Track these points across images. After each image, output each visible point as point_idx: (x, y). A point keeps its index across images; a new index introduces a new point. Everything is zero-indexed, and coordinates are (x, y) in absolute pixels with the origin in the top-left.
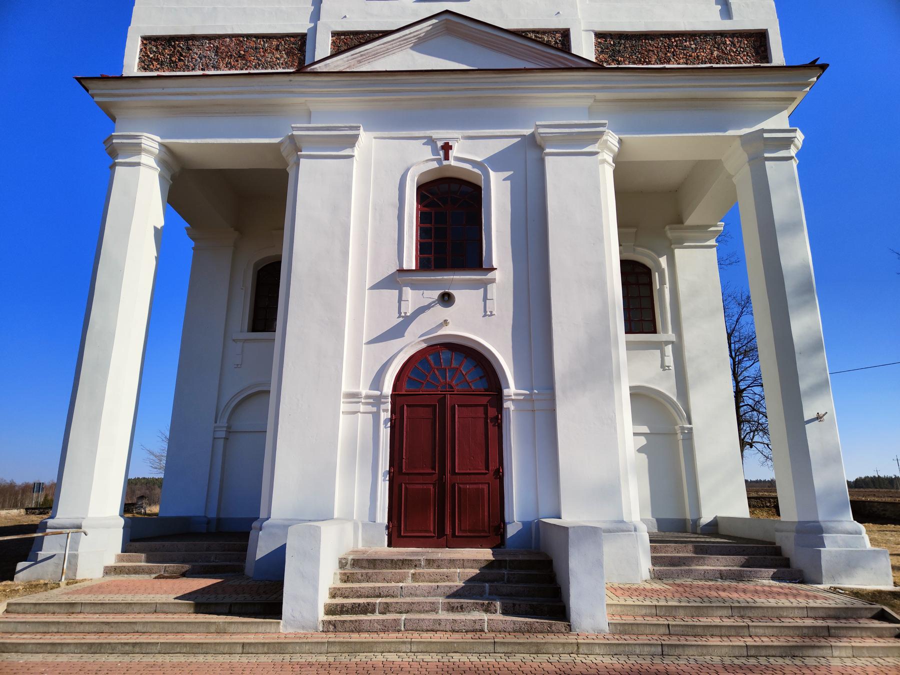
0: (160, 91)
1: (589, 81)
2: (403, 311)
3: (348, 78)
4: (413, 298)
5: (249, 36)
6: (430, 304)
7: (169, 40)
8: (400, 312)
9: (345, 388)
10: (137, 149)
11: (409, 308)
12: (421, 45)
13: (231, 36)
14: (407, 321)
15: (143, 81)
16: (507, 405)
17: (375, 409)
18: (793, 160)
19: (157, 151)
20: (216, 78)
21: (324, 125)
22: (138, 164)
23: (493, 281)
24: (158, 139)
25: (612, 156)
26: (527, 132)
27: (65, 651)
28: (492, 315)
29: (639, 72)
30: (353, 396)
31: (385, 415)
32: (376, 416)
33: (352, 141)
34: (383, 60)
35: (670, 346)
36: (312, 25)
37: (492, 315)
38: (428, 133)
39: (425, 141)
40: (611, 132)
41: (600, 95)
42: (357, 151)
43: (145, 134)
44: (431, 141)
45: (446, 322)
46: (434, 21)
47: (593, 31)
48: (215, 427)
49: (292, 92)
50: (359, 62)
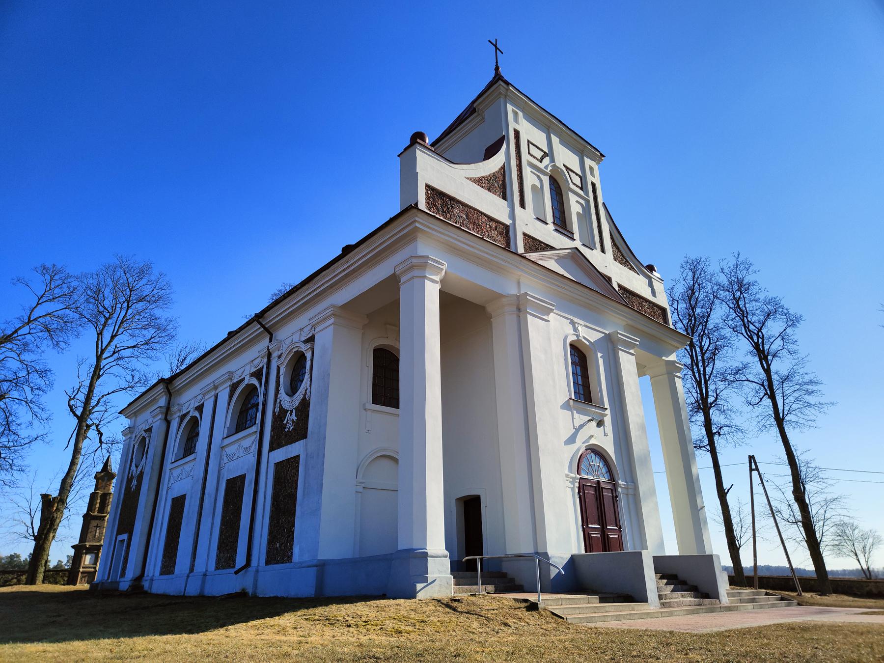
0: (456, 237)
2: (575, 425)
3: (545, 271)
4: (580, 419)
5: (482, 213)
6: (584, 424)
7: (441, 195)
8: (574, 426)
11: (577, 425)
12: (560, 260)
13: (474, 209)
14: (577, 430)
16: (620, 490)
17: (572, 486)
20: (488, 243)
21: (533, 295)
23: (606, 415)
26: (607, 332)
27: (609, 619)
28: (607, 436)
29: (637, 314)
31: (577, 490)
32: (573, 489)
33: (548, 311)
34: (547, 262)
36: (511, 222)
37: (607, 436)
38: (576, 320)
39: (570, 321)
44: (572, 323)
45: (592, 436)
46: (569, 251)
48: (357, 482)
49: (518, 268)
50: (540, 259)
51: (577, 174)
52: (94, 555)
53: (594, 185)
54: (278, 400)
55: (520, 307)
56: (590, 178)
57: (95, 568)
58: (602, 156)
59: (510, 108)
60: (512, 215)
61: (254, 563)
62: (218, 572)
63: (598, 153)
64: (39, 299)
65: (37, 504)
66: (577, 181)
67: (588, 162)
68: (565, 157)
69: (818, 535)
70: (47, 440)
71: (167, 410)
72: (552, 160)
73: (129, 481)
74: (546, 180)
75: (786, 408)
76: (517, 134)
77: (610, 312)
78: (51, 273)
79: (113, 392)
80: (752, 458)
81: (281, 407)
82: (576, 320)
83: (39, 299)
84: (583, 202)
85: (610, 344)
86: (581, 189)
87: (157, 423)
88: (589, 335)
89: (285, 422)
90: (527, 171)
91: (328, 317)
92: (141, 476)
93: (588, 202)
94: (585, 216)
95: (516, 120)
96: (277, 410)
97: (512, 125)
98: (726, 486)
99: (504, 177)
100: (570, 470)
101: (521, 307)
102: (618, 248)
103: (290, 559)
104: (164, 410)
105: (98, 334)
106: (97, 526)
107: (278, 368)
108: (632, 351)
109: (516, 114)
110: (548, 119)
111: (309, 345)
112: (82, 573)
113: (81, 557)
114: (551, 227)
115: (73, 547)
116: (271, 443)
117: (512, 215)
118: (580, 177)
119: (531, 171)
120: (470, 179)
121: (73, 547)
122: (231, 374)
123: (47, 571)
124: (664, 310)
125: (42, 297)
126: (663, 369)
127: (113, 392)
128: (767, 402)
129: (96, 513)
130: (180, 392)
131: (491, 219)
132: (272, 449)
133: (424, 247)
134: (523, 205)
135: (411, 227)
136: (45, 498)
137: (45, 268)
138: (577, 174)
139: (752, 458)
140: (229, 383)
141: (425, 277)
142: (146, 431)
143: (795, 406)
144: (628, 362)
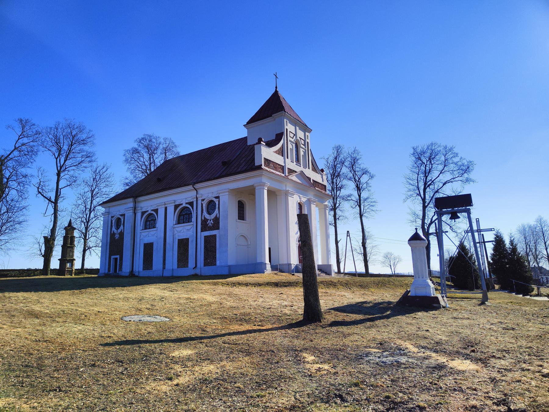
13: (275, 163)
33: (293, 195)
44: (299, 196)
51: (303, 140)
52: (71, 263)
53: (308, 142)
54: (203, 215)
55: (287, 194)
56: (307, 140)
57: (72, 269)
58: (311, 130)
59: (285, 120)
60: (285, 162)
61: (198, 265)
62: (178, 269)
64: (19, 137)
65: (42, 240)
66: (303, 142)
67: (307, 134)
68: (300, 134)
69: (368, 258)
70: (27, 209)
71: (135, 209)
72: (296, 137)
73: (113, 235)
74: (294, 145)
75: (364, 211)
76: (287, 129)
78: (23, 123)
79: (64, 187)
80: (348, 232)
81: (204, 217)
82: (300, 195)
83: (19, 137)
84: (304, 150)
85: (309, 202)
86: (304, 145)
87: (129, 214)
88: (304, 200)
89: (208, 223)
90: (289, 143)
91: (226, 192)
92: (122, 234)
93: (305, 150)
94: (304, 156)
95: (287, 125)
96: (203, 218)
97: (286, 127)
98: (338, 239)
99: (283, 148)
100: (296, 242)
101: (287, 194)
102: (313, 165)
103: (215, 265)
104: (133, 209)
105: (57, 159)
106: (71, 251)
107: (202, 204)
108: (315, 204)
109: (286, 121)
111: (217, 200)
112: (67, 271)
113: (66, 264)
114: (295, 163)
115: (59, 260)
116: (201, 229)
117: (285, 162)
118: (304, 141)
121: (59, 260)
122: (175, 201)
123: (51, 270)
124: (325, 186)
125: (20, 136)
126: (323, 207)
127: (64, 187)
128: (358, 208)
129: (69, 245)
130: (139, 202)
131: (279, 165)
132: (202, 231)
133: (264, 180)
134: (288, 158)
135: (261, 174)
136: (45, 238)
137: (21, 121)
138: (303, 140)
139: (348, 232)
140: (173, 204)
141: (264, 189)
142: (121, 215)
143: (368, 210)
144: (313, 207)
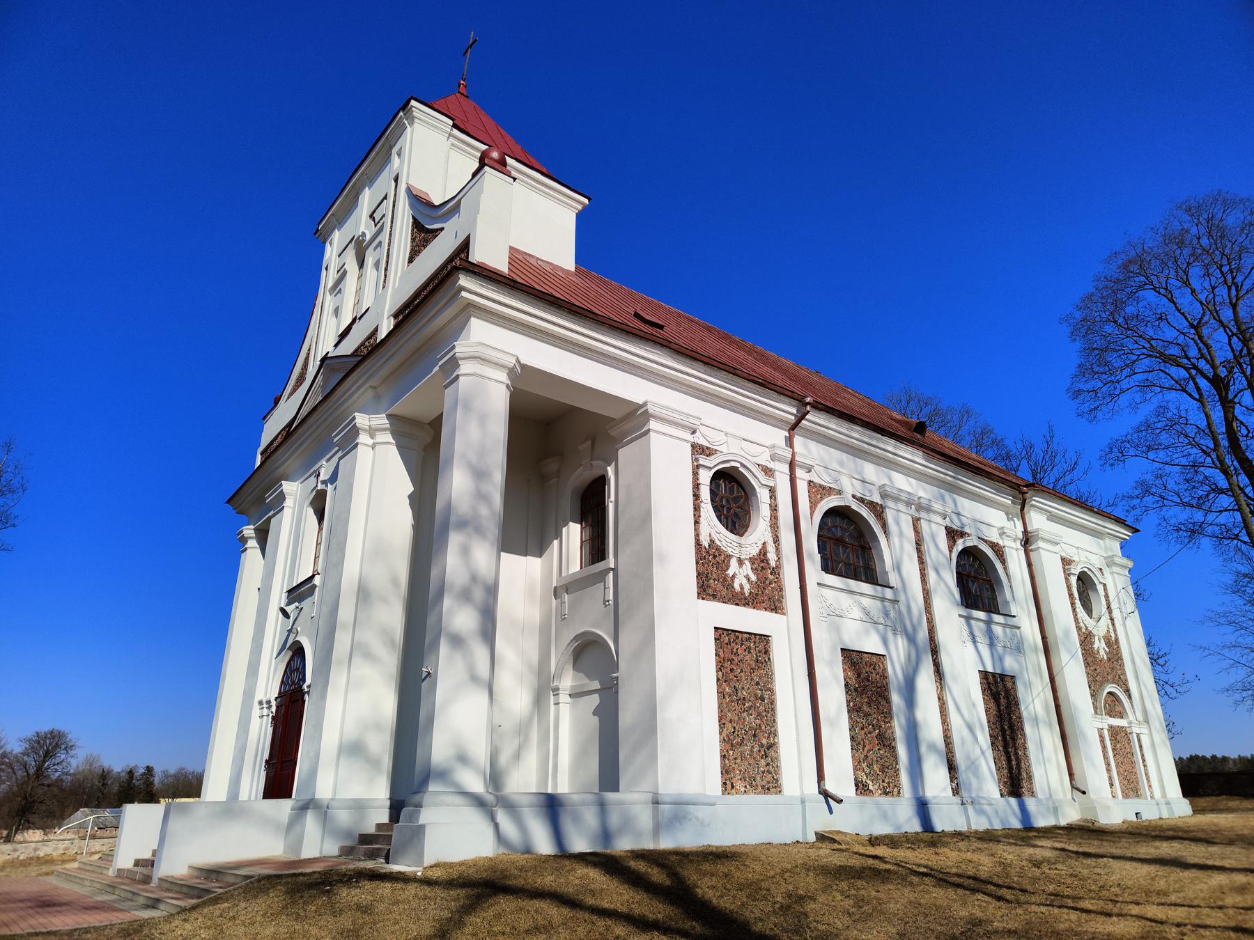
1: (360, 378)
9: (257, 699)
10: (244, 540)
15: (241, 491)
18: (460, 378)
19: (254, 535)
22: (246, 549)
24: (252, 527)
25: (389, 432)
30: (261, 703)
35: (611, 575)
40: (371, 416)
41: (371, 383)
42: (289, 503)
43: (244, 528)
47: (391, 315)
63: (401, 113)
77: (341, 410)
110: (350, 191)
119: (335, 296)
120: (288, 398)
